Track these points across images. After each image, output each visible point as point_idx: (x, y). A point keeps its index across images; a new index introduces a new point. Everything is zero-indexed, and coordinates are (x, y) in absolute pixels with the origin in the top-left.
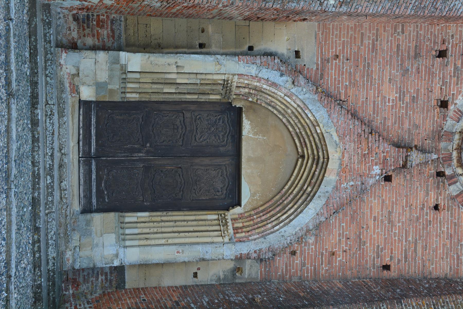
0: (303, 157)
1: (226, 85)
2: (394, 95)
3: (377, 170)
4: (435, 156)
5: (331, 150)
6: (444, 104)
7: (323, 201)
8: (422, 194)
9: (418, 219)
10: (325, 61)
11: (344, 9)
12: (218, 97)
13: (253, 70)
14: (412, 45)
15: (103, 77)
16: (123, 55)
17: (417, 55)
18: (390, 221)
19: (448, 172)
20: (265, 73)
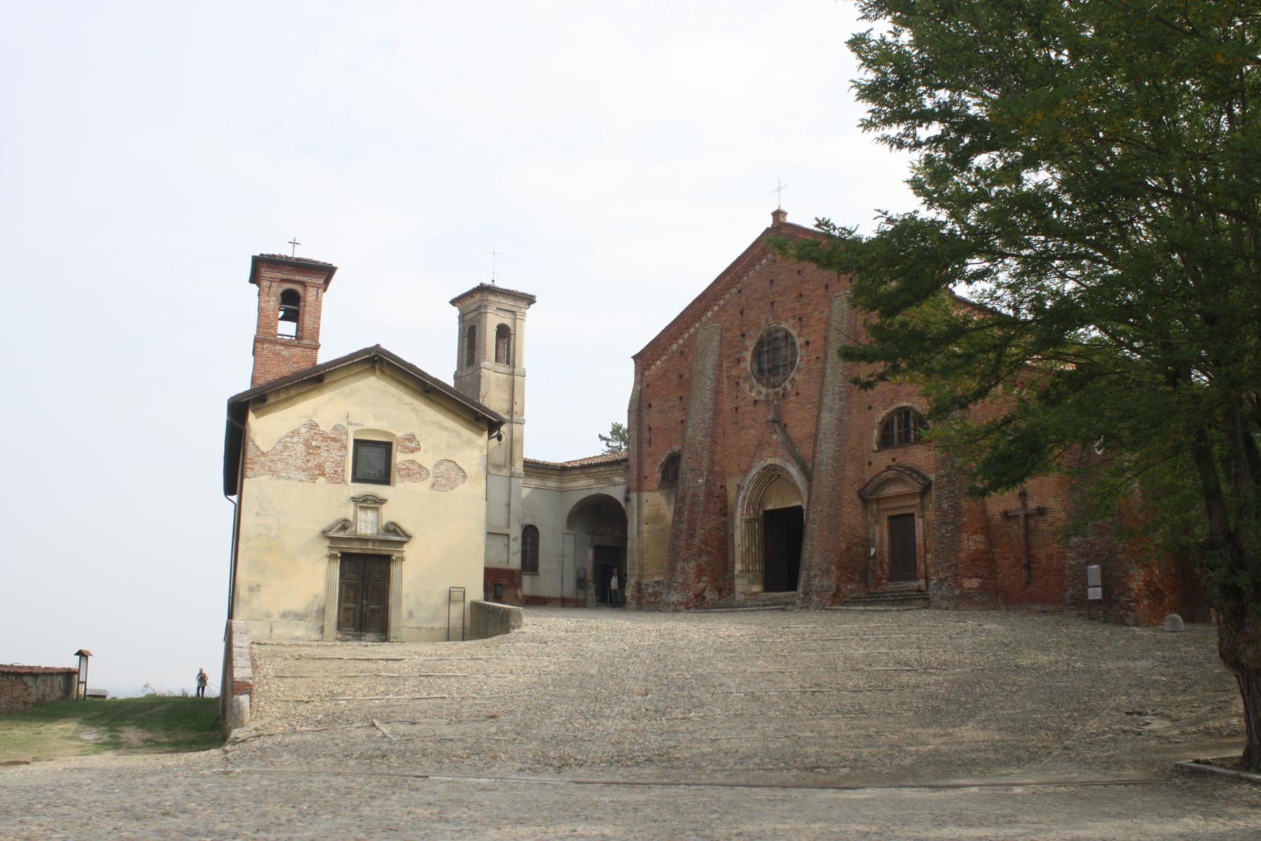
0: (779, 476)
1: (748, 522)
2: (752, 431)
3: (774, 437)
4: (776, 402)
5: (767, 464)
6: (756, 402)
7: (787, 463)
8: (792, 405)
9: (802, 404)
10: (741, 471)
11: (705, 473)
12: (757, 525)
13: (739, 509)
14: (733, 426)
15: (745, 581)
16: (736, 572)
17: (736, 423)
18: (803, 420)
19: (782, 392)
20: (740, 504)
